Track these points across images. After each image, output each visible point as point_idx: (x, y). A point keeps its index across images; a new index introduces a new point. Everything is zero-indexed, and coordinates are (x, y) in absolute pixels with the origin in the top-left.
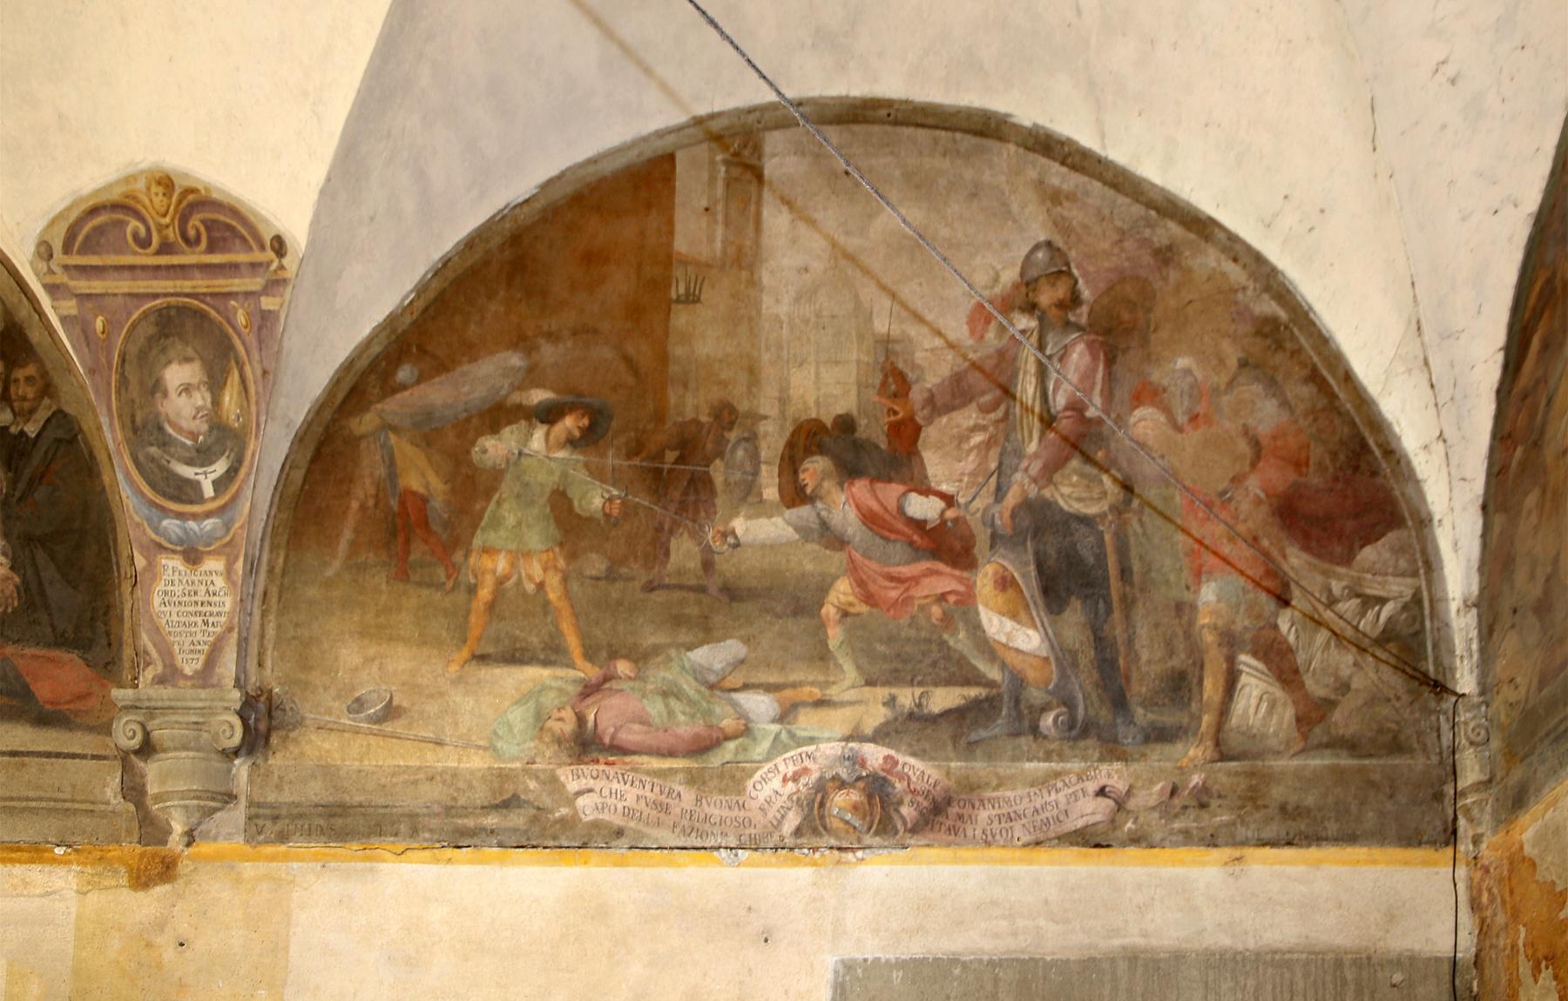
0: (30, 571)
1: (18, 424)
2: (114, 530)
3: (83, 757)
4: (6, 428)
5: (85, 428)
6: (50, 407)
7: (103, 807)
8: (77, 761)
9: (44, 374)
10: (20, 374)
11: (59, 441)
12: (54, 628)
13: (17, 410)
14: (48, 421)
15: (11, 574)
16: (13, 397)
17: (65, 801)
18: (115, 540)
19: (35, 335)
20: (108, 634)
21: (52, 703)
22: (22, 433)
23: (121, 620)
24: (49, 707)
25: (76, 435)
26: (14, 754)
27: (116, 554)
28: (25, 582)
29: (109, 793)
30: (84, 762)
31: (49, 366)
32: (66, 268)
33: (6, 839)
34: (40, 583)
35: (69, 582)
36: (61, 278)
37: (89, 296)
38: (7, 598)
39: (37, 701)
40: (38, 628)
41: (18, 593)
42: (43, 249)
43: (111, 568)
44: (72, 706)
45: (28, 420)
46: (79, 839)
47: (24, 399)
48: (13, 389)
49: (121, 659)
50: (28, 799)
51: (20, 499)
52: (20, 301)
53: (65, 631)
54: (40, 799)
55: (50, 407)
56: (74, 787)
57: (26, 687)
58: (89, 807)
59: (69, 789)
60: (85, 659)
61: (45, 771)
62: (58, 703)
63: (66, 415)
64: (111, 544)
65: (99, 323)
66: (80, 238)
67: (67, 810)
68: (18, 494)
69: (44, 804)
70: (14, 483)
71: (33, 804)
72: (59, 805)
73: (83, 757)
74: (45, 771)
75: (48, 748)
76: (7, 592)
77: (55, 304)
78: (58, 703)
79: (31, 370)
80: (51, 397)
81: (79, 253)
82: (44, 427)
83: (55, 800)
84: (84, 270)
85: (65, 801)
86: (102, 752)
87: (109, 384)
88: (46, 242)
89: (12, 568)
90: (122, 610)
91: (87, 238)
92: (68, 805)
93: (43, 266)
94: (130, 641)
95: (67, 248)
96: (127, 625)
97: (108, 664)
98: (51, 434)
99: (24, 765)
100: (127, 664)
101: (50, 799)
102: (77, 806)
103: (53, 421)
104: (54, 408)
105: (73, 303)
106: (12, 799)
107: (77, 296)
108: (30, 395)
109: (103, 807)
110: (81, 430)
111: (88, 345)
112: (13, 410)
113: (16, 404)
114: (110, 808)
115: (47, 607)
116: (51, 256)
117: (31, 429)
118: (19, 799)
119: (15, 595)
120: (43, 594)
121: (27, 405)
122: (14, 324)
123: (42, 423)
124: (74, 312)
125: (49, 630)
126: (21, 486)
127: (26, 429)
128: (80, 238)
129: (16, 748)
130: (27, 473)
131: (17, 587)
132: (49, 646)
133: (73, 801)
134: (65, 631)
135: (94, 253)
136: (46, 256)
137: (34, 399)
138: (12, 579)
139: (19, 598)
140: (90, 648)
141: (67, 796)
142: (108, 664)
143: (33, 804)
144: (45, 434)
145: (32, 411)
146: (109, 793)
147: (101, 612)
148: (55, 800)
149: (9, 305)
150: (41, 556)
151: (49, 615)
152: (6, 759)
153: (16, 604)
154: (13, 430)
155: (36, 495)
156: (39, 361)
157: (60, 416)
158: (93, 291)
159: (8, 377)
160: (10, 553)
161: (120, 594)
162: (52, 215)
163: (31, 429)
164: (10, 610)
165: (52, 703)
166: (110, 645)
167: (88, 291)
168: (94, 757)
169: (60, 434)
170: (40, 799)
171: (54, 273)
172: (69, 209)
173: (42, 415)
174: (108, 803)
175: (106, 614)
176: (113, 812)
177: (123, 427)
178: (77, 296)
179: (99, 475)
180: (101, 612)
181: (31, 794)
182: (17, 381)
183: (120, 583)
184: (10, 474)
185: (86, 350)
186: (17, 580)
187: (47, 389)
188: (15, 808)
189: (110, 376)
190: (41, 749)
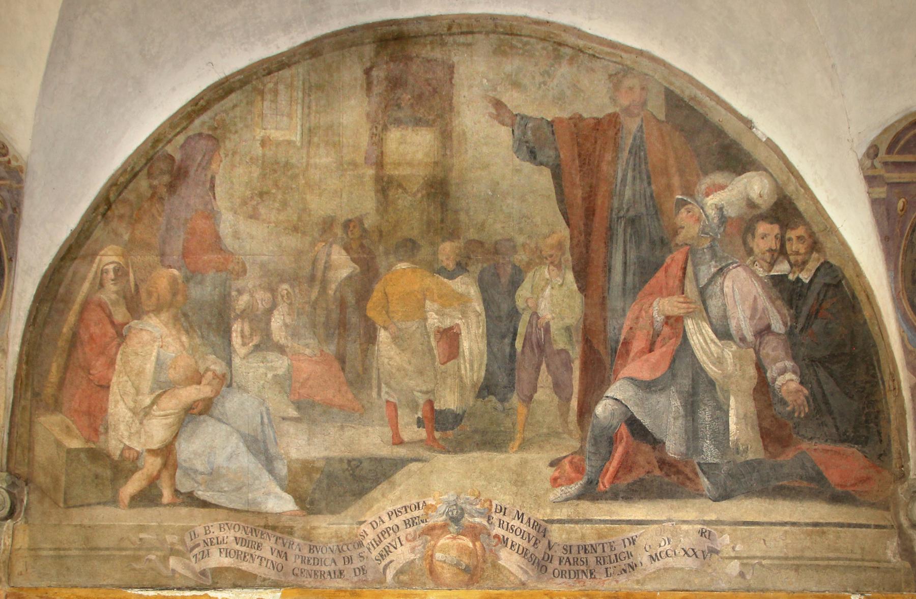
0: (815, 385)
1: (794, 273)
2: (877, 353)
3: (868, 526)
4: (786, 276)
5: (847, 276)
6: (819, 259)
7: (885, 565)
8: (864, 529)
9: (812, 235)
10: (792, 234)
11: (827, 285)
12: (837, 429)
13: (793, 262)
14: (818, 269)
15: (801, 387)
16: (789, 252)
17: (857, 560)
18: (878, 361)
19: (801, 205)
20: (879, 433)
21: (841, 486)
22: (798, 280)
23: (889, 422)
24: (839, 489)
25: (840, 281)
26: (816, 525)
27: (880, 372)
28: (812, 394)
29: (889, 554)
30: (869, 530)
31: (815, 229)
32: (886, 164)
33: (814, 589)
34: (824, 395)
35: (847, 394)
36: (880, 171)
37: (898, 184)
38: (800, 406)
39: (830, 485)
40: (826, 429)
41: (808, 402)
42: (871, 151)
43: (877, 383)
44: (856, 488)
45: (802, 270)
46: (870, 589)
47: (797, 253)
48: (788, 246)
49: (890, 451)
50: (829, 559)
51: (802, 330)
52: (788, 179)
53: (846, 431)
54: (838, 559)
55: (819, 259)
56: (863, 549)
57: (819, 473)
58: (875, 564)
59: (859, 551)
60: (863, 452)
61: (839, 537)
62: (845, 486)
63: (831, 266)
64: (876, 364)
65: (900, 204)
66: (902, 142)
67: (859, 567)
68: (800, 326)
69: (841, 563)
70: (796, 317)
71: (833, 563)
72: (853, 563)
73: (868, 526)
74: (839, 537)
75: (841, 520)
76: (799, 402)
77: (871, 190)
78: (845, 486)
79: (801, 231)
80: (818, 251)
81: (899, 153)
82: (815, 275)
83: (850, 560)
84: (898, 165)
85: (857, 560)
86: (882, 523)
87: (899, 248)
88: (876, 146)
89: (801, 383)
90: (889, 414)
91: (908, 142)
92: (859, 563)
93: (868, 163)
94: (896, 438)
95: (890, 150)
96: (894, 425)
97: (881, 455)
98: (820, 281)
99: (824, 533)
100: (895, 455)
101: (846, 559)
102: (866, 564)
103: (822, 270)
104: (822, 260)
105: (884, 189)
106: (816, 559)
107: (888, 184)
108: (802, 251)
109: (885, 565)
110: (844, 277)
111: (888, 219)
112: (789, 262)
113: (792, 258)
114: (891, 566)
115: (831, 413)
116: (876, 155)
117: (805, 277)
118: (822, 559)
119: (805, 403)
120: (827, 403)
121: (800, 258)
122: (785, 197)
123: (813, 271)
124: (883, 196)
125: (834, 430)
126: (802, 320)
127: (801, 276)
128: (902, 142)
129: (816, 520)
130: (805, 310)
131: (807, 398)
132: (835, 441)
133: (863, 560)
134: (846, 431)
135: (910, 153)
136: (872, 156)
137: (806, 253)
138: (802, 391)
139: (809, 406)
140: (866, 443)
141: (858, 556)
142: (881, 455)
143: (833, 563)
144: (816, 280)
145: (804, 263)
146: (889, 554)
147: (873, 416)
148: (850, 560)
149: (780, 182)
150: (822, 374)
151: (833, 418)
152: (810, 528)
153: (807, 410)
154: (791, 277)
155: (813, 326)
156: (807, 225)
157: (826, 266)
158: (902, 181)
159: (783, 237)
160: (798, 371)
161: (886, 402)
162: (886, 126)
163: (805, 277)
164: (802, 415)
165: (841, 486)
166: (881, 441)
167: (898, 181)
168: (877, 527)
169: (828, 280)
170: (838, 559)
171: (875, 168)
172: (899, 121)
173: (812, 266)
174: (889, 562)
175: (876, 418)
176: (894, 568)
177: (904, 280)
178: (888, 184)
179: (860, 311)
180: (873, 416)
181: (831, 555)
182: (790, 239)
183: (885, 394)
184: (792, 311)
185: (886, 223)
186: (806, 392)
187: (815, 246)
188: (819, 565)
189: (901, 242)
190: (836, 521)
